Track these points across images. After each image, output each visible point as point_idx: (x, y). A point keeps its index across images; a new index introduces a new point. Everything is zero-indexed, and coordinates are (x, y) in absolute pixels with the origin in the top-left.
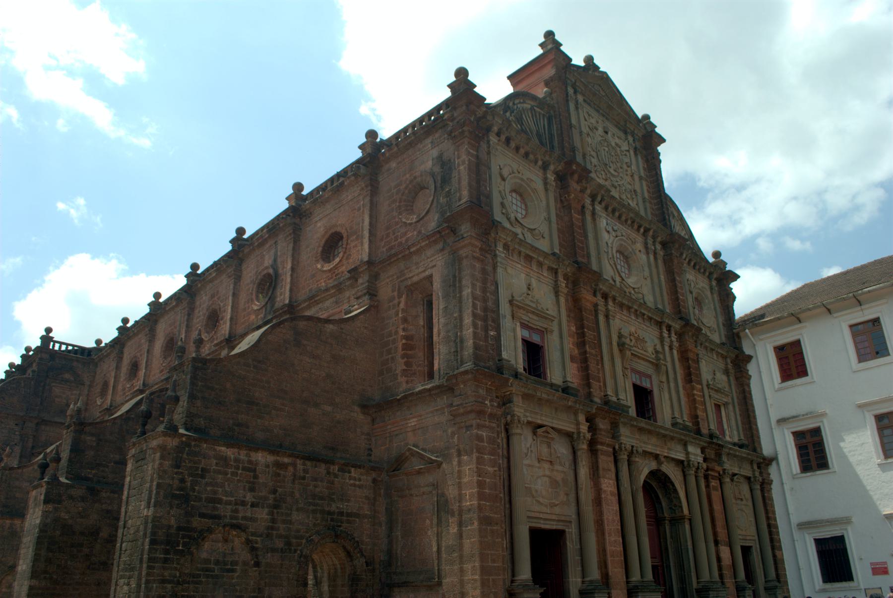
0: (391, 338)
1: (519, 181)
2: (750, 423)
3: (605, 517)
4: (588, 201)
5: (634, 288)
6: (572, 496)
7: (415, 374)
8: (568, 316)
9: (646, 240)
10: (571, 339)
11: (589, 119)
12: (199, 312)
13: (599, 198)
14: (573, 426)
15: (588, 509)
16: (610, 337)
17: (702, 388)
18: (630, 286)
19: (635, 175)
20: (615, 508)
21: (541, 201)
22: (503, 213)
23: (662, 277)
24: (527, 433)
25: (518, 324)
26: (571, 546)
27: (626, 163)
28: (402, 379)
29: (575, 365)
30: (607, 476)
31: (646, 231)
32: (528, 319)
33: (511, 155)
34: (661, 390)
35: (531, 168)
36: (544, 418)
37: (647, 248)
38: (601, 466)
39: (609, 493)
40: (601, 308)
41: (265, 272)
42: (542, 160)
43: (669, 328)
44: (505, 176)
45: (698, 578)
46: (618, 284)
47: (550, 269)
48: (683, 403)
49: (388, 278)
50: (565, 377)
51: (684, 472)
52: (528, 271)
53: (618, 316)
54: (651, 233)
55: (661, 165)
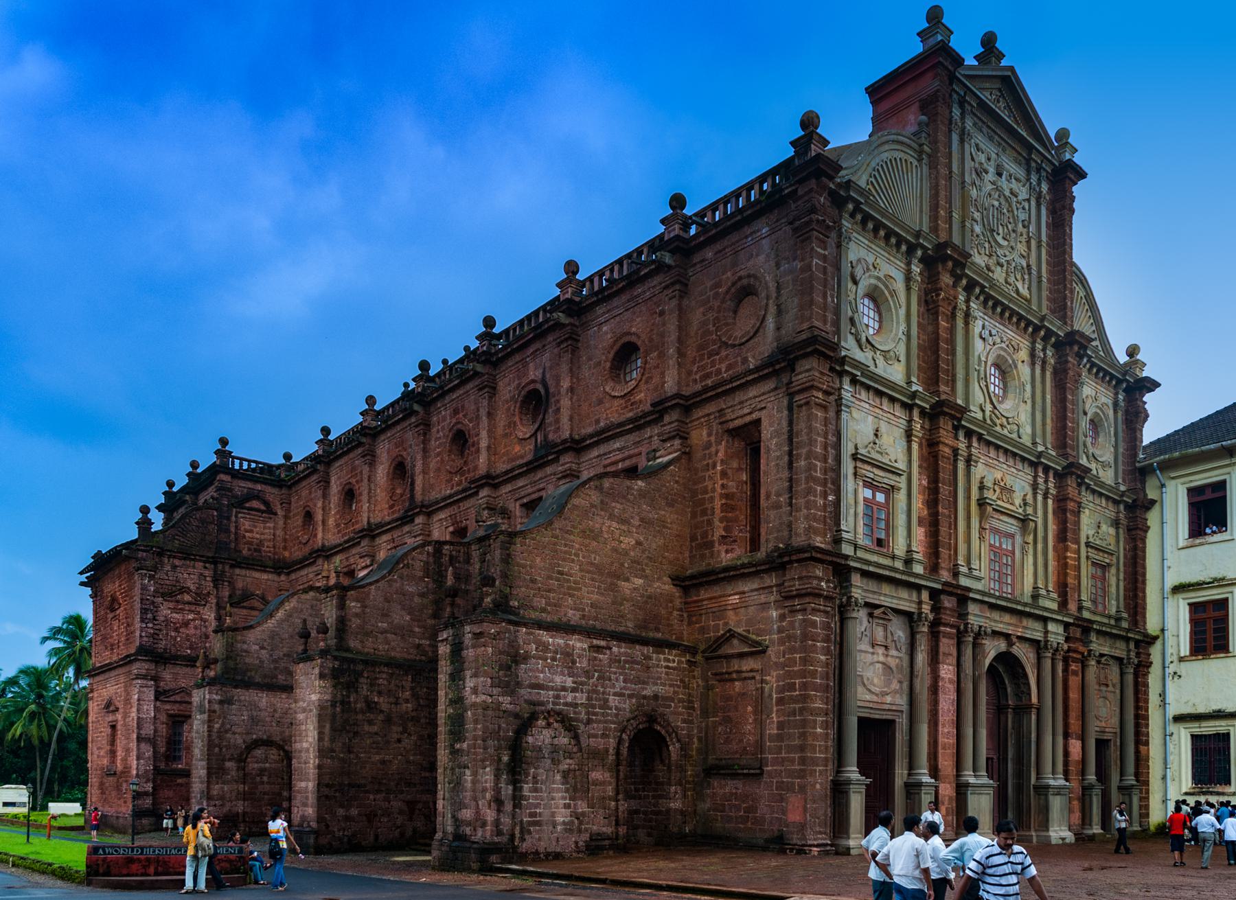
0: (707, 496)
2: (1135, 589)
7: (735, 541)
8: (920, 466)
10: (921, 497)
12: (438, 432)
17: (1079, 547)
24: (862, 614)
25: (861, 484)
28: (723, 548)
32: (871, 475)
36: (882, 598)
40: (963, 451)
41: (532, 387)
46: (988, 413)
49: (703, 417)
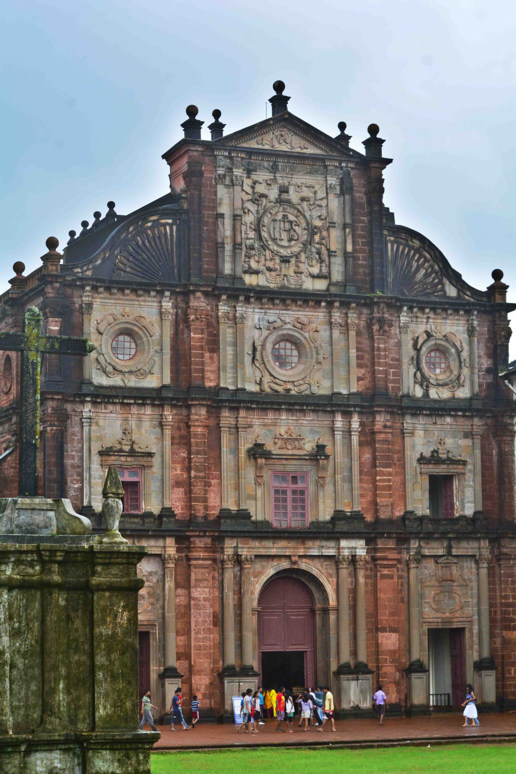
1: (125, 326)
3: (193, 620)
4: (223, 308)
5: (293, 382)
6: (160, 603)
9: (330, 313)
11: (253, 188)
13: (242, 298)
14: (160, 549)
15: (171, 615)
16: (236, 451)
18: (285, 382)
19: (332, 230)
20: (208, 611)
21: (151, 336)
22: (99, 369)
23: (353, 353)
26: (154, 643)
27: (320, 216)
29: (182, 489)
30: (201, 585)
31: (330, 305)
33: (113, 301)
34: (320, 483)
35: (142, 303)
37: (331, 323)
38: (193, 577)
39: (202, 599)
42: (154, 290)
43: (347, 414)
44: (101, 331)
45: (338, 663)
47: (153, 405)
48: (356, 492)
50: (163, 505)
51: (337, 566)
52: (125, 416)
53: (256, 422)
54: (337, 304)
55: (384, 195)
